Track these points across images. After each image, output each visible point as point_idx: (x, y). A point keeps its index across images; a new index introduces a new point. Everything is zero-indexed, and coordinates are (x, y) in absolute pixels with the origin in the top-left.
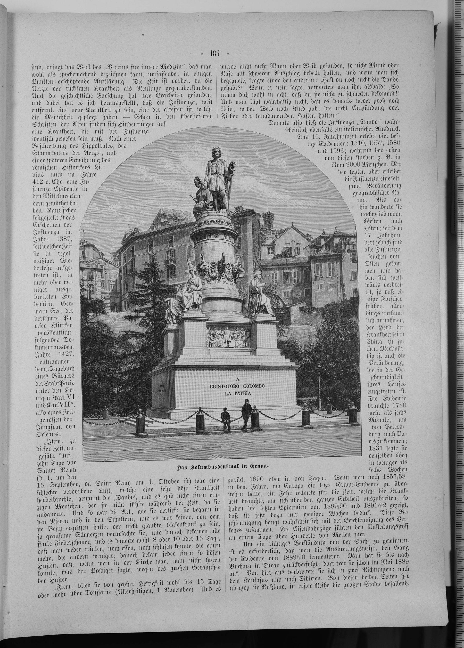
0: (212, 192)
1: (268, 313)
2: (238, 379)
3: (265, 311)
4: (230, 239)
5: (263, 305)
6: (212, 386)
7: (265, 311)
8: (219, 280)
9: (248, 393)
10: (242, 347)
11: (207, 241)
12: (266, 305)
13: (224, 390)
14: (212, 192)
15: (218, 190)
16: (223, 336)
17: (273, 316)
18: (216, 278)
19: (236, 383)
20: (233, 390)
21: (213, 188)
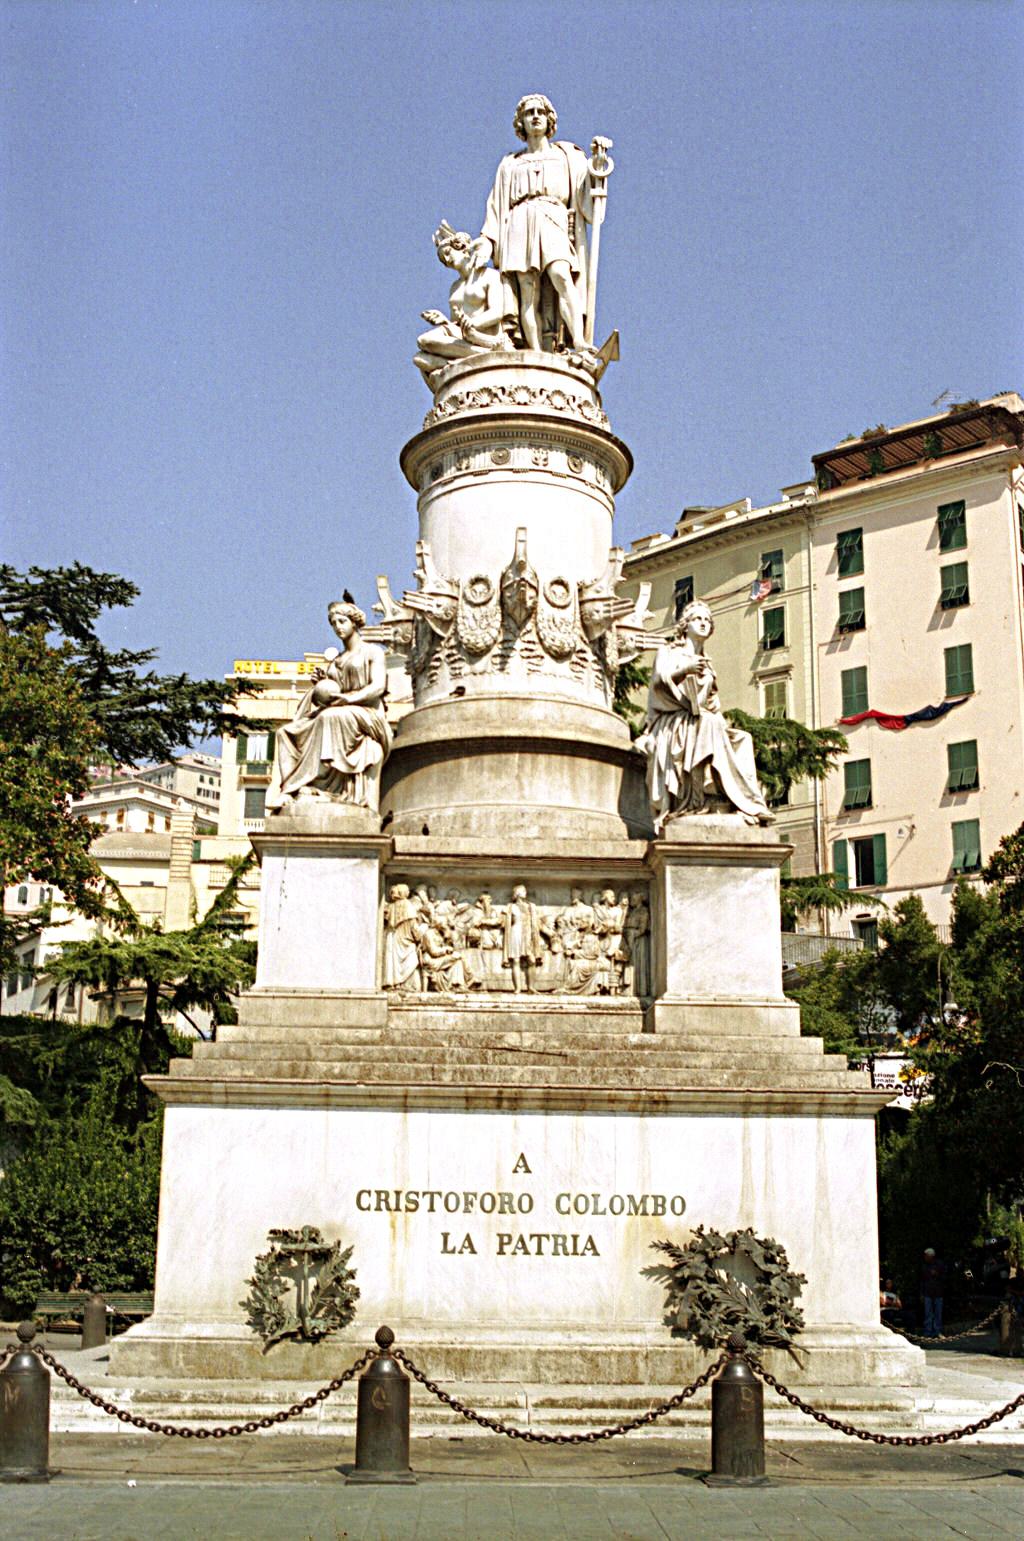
1: (733, 808)
2: (523, 1164)
3: (720, 800)
6: (372, 1201)
7: (720, 800)
8: (504, 657)
9: (582, 1243)
10: (604, 991)
13: (442, 1220)
14: (512, 277)
15: (536, 263)
16: (503, 931)
18: (488, 649)
19: (517, 1185)
20: (483, 1227)
21: (515, 262)
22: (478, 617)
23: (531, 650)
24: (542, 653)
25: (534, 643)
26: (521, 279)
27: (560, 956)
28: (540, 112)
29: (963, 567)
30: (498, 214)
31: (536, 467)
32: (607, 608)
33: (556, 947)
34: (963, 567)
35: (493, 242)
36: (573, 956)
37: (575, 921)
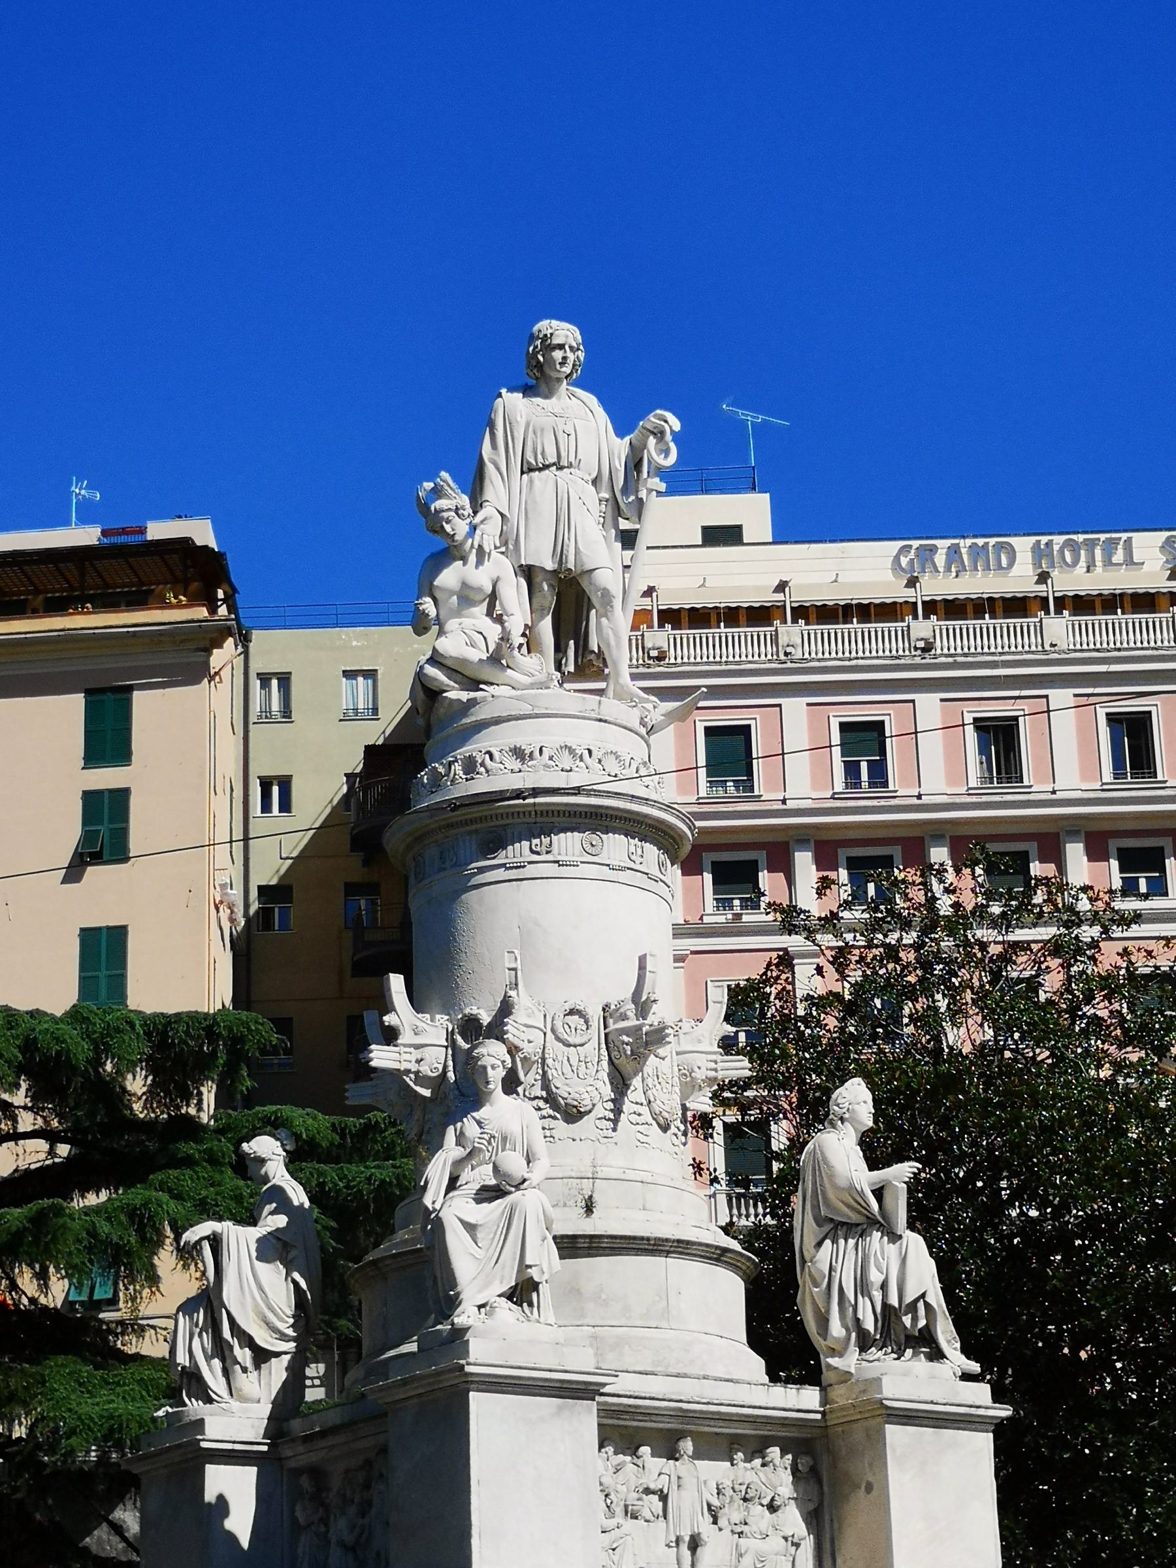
0: (528, 573)
4: (661, 865)
5: (917, 1300)
11: (530, 871)
12: (930, 1299)
16: (664, 1498)
17: (966, 1377)
22: (574, 1062)
23: (639, 1115)
24: (651, 1120)
25: (642, 1104)
26: (538, 578)
27: (727, 1532)
28: (571, 348)
29: (121, 796)
30: (506, 480)
31: (632, 865)
32: (713, 1065)
33: (722, 1522)
34: (121, 796)
35: (502, 515)
36: (740, 1534)
37: (737, 1487)
